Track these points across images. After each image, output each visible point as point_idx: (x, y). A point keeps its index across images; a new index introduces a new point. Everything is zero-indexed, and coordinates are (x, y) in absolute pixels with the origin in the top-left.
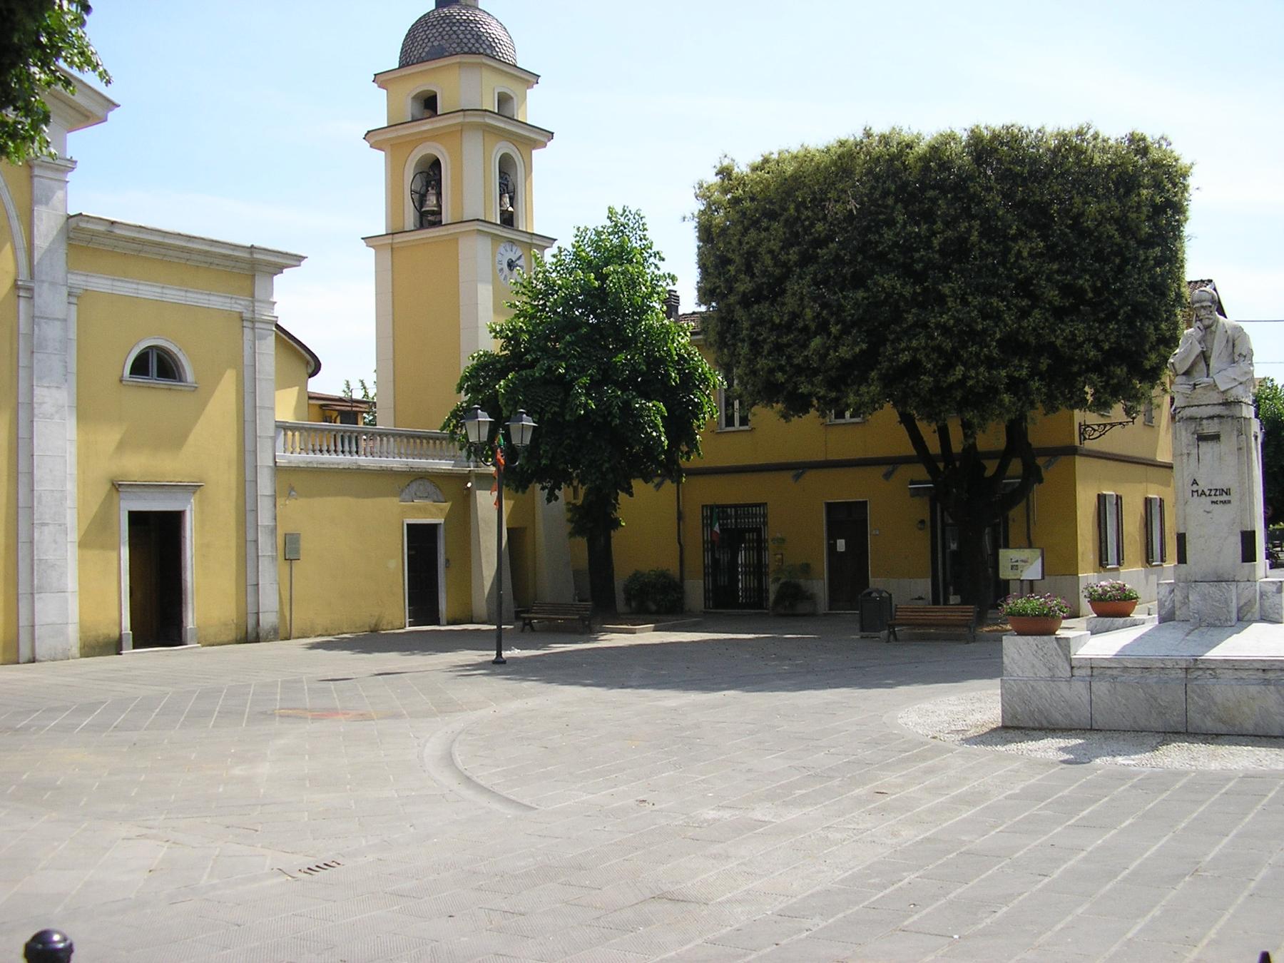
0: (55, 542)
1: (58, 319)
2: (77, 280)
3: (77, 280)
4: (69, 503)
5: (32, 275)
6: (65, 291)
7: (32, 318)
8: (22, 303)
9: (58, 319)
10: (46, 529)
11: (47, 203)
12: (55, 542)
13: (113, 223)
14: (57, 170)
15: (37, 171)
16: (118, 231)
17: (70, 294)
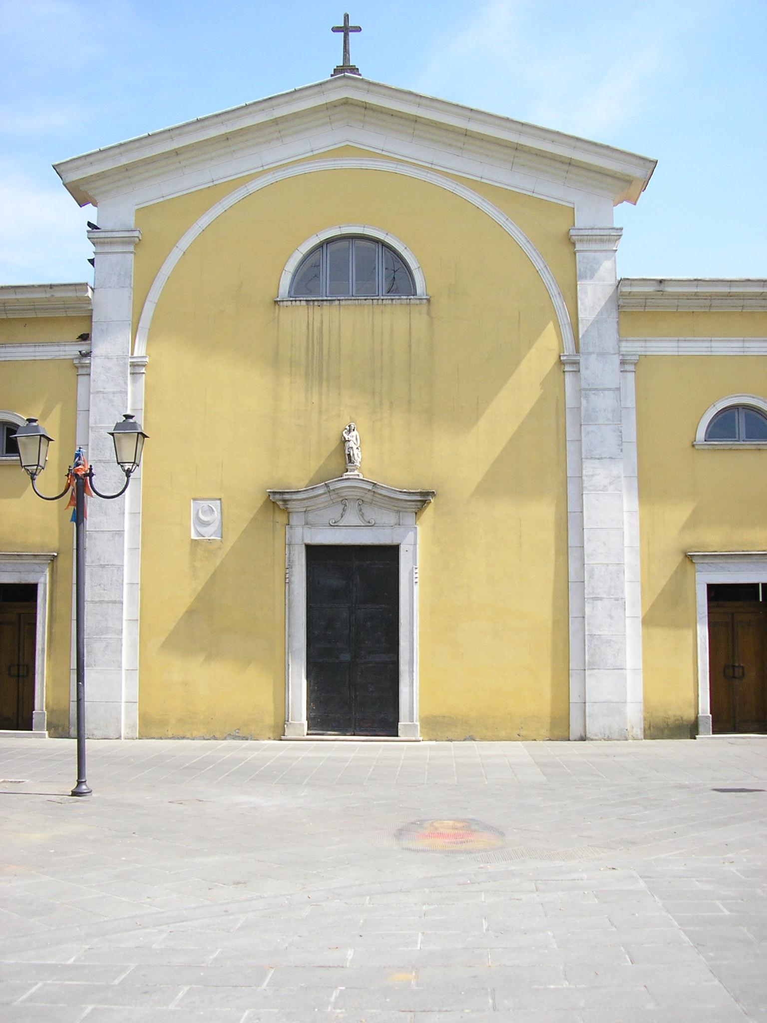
0: (611, 617)
1: (609, 389)
2: (633, 347)
3: (633, 347)
4: (627, 576)
5: (577, 351)
6: (616, 360)
7: (580, 392)
8: (568, 378)
9: (609, 389)
10: (599, 604)
11: (592, 277)
12: (611, 617)
13: (661, 281)
14: (602, 241)
15: (578, 247)
16: (669, 289)
17: (623, 363)
